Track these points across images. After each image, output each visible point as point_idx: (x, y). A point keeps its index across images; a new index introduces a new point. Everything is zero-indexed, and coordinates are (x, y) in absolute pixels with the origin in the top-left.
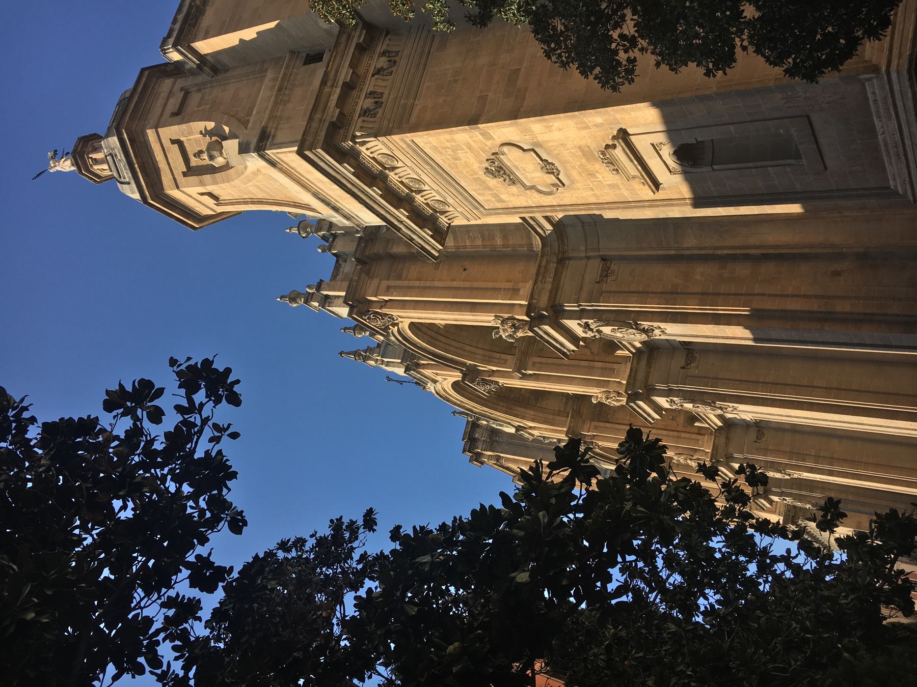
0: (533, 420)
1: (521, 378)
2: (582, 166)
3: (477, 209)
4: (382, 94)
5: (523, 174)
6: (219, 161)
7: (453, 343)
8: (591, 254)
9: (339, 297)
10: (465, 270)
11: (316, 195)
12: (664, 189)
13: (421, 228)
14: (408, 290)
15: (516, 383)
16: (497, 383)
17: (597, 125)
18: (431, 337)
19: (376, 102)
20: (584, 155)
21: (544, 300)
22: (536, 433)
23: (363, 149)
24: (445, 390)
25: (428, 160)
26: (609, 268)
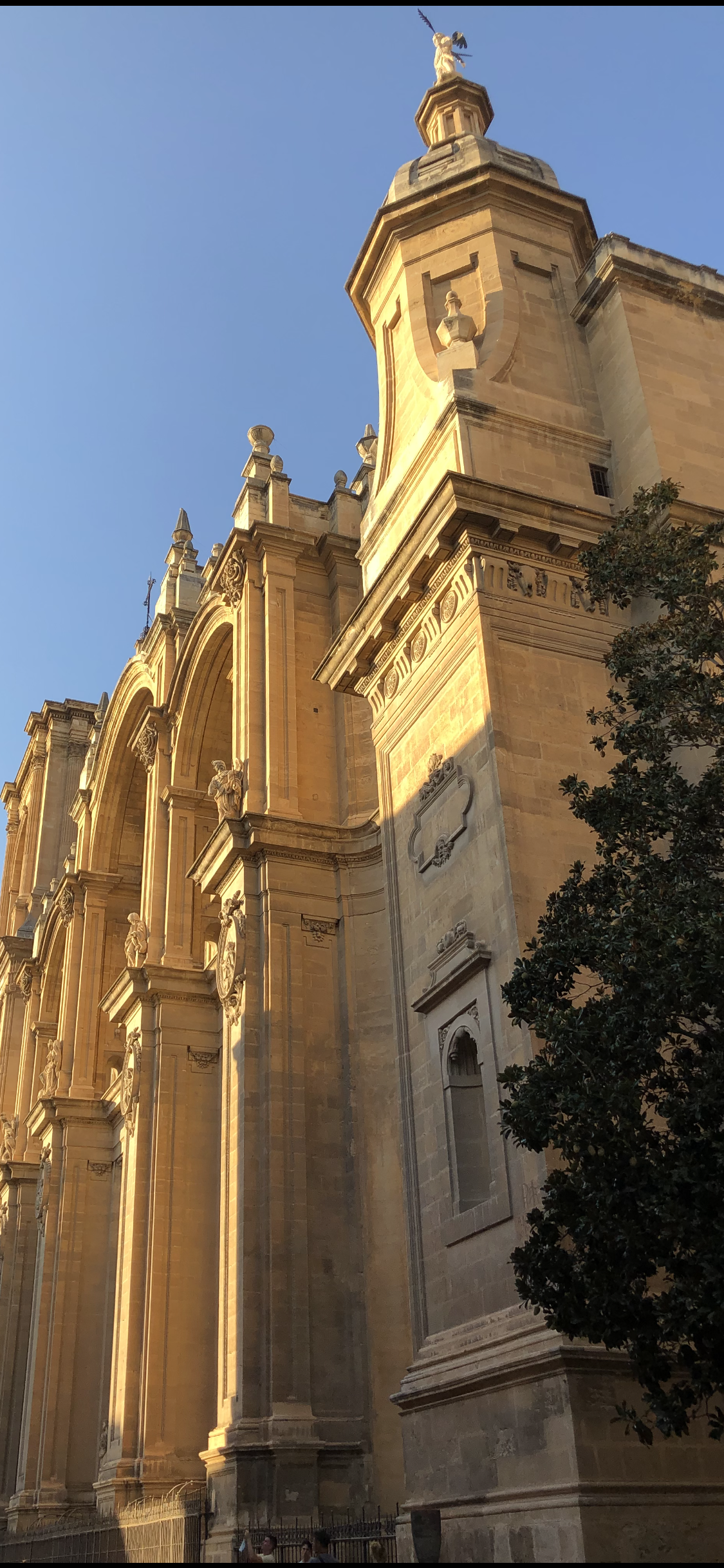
0: (101, 816)
3: (388, 741)
4: (543, 594)
6: (444, 335)
8: (345, 902)
9: (266, 511)
10: (316, 710)
11: (401, 490)
12: (421, 1019)
13: (357, 657)
14: (280, 623)
15: (153, 794)
17: (498, 920)
19: (530, 587)
21: (271, 838)
22: (81, 823)
23: (462, 571)
24: (137, 676)
25: (450, 667)
26: (325, 932)
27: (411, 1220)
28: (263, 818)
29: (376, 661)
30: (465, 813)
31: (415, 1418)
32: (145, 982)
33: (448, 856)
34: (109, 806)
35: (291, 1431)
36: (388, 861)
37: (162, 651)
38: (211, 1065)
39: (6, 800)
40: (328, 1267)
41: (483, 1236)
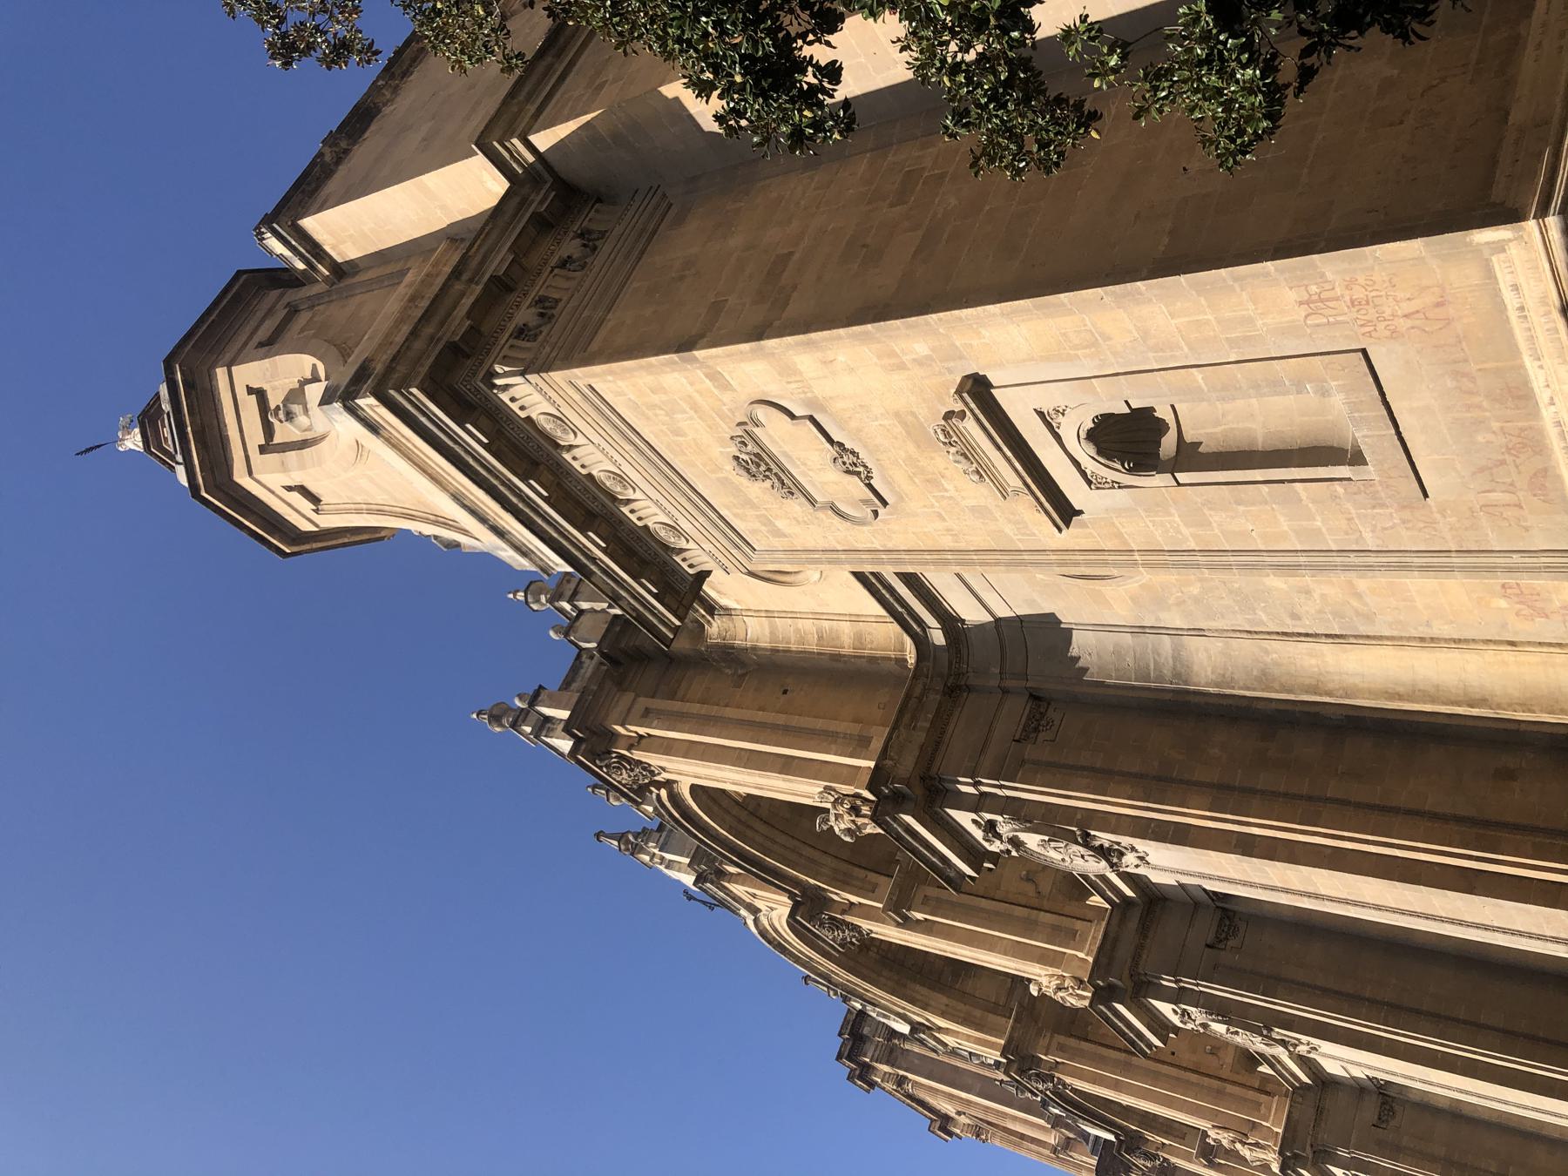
0: (943, 1015)
1: (898, 925)
5: (804, 474)
7: (782, 839)
8: (1009, 683)
10: (785, 692)
11: (458, 498)
12: (1084, 525)
13: (634, 578)
16: (856, 928)
17: (920, 362)
18: (740, 821)
20: (908, 433)
21: (907, 764)
24: (776, 930)
26: (1043, 715)
27: (1388, 567)
30: (792, 416)
33: (853, 453)
36: (881, 562)
37: (738, 889)
39: (951, 1134)
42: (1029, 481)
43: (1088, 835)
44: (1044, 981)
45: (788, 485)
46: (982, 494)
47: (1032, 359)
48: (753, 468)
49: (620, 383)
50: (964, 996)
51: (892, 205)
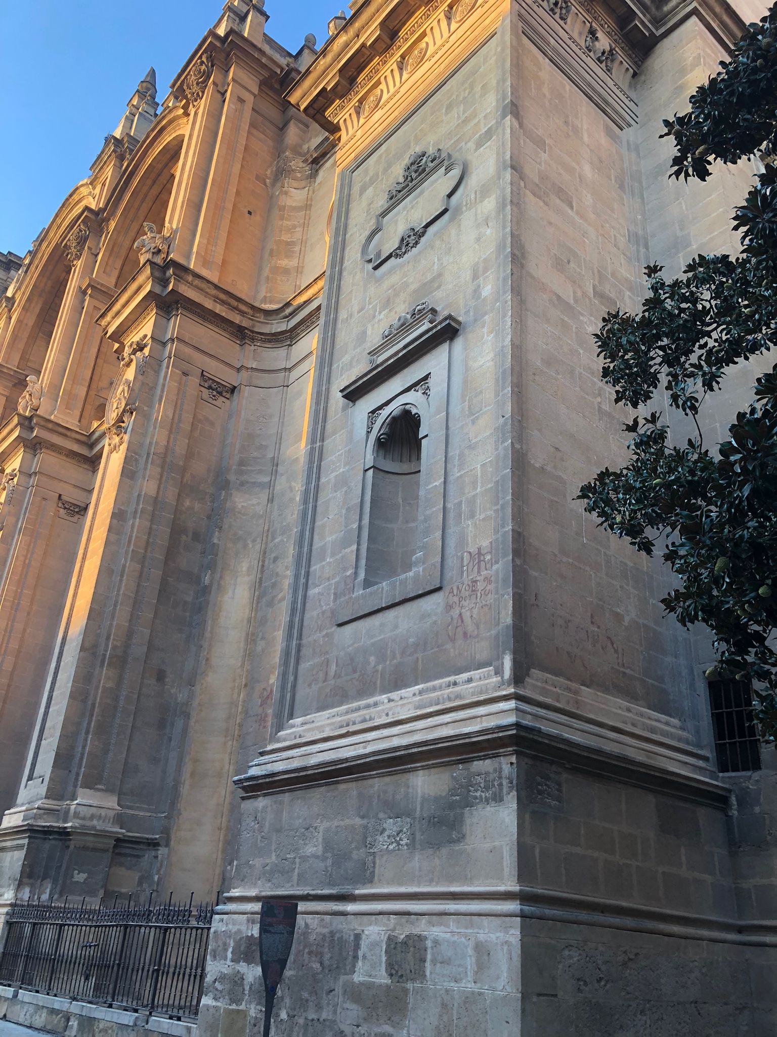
0: (19, 321)
2: (406, 285)
5: (404, 209)
10: (250, 213)
12: (345, 408)
13: (340, 70)
17: (477, 292)
20: (425, 284)
26: (220, 393)
27: (294, 602)
28: (186, 270)
29: (359, 80)
30: (450, 196)
31: (261, 803)
32: (31, 429)
33: (417, 243)
34: (28, 314)
35: (92, 817)
38: (77, 516)
40: (161, 676)
41: (391, 614)
42: (380, 369)
43: (132, 413)
44: (37, 386)
45: (396, 197)
46: (374, 338)
47: (467, 371)
48: (414, 167)
49: (494, 58)
50: (32, 338)
51: (594, 287)
